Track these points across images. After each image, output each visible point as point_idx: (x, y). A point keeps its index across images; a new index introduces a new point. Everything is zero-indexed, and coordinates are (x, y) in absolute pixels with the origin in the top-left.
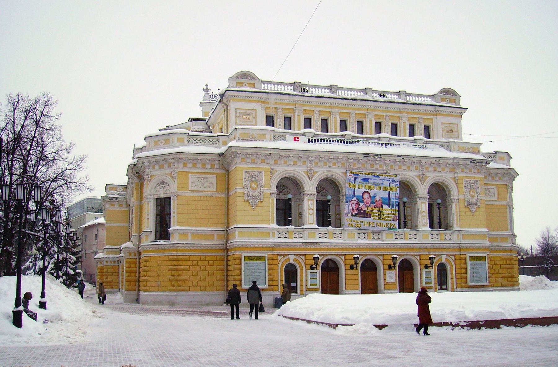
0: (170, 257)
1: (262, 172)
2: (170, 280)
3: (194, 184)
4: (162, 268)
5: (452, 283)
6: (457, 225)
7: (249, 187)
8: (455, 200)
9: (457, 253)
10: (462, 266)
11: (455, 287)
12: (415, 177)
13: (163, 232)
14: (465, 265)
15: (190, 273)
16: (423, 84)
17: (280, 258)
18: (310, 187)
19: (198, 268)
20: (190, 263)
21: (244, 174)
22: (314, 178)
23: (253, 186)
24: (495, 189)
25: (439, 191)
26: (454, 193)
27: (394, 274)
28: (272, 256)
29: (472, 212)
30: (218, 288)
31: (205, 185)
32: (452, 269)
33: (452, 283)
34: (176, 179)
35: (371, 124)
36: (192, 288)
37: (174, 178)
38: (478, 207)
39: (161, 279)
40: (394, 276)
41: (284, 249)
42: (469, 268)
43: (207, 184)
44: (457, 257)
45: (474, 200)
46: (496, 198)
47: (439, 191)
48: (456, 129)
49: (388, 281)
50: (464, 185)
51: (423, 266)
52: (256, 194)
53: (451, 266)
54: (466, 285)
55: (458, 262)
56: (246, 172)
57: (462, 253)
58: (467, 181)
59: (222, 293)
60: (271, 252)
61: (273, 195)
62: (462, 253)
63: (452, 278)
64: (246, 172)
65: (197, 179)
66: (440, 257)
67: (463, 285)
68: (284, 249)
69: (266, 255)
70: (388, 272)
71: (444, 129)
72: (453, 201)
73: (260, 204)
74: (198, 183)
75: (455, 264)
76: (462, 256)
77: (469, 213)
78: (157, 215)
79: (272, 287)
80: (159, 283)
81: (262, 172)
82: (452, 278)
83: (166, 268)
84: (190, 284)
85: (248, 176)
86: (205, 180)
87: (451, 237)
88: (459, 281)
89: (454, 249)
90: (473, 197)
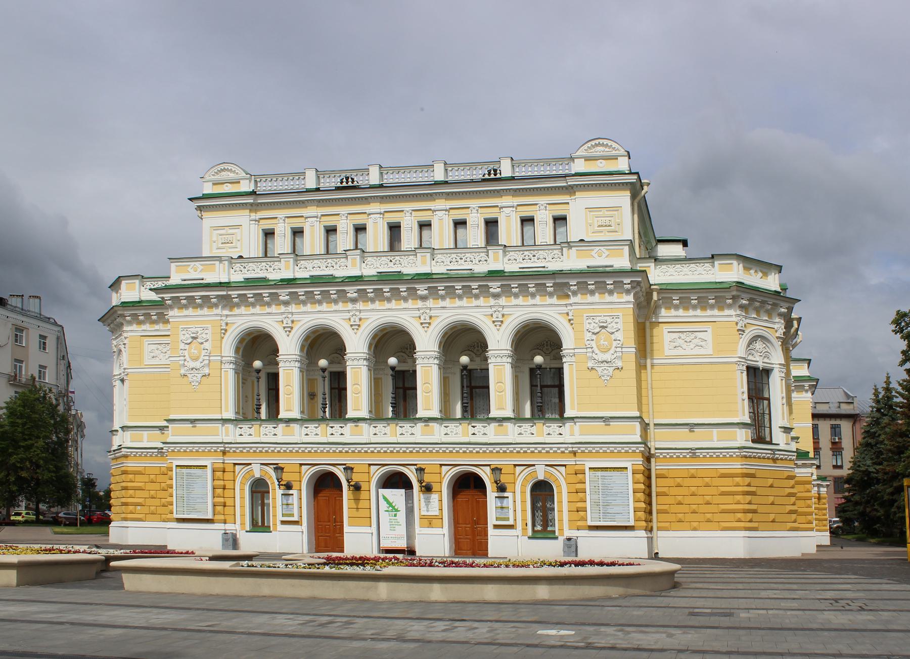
12: (483, 318)
24: (710, 330)
26: (568, 342)
58: (593, 317)
61: (227, 366)
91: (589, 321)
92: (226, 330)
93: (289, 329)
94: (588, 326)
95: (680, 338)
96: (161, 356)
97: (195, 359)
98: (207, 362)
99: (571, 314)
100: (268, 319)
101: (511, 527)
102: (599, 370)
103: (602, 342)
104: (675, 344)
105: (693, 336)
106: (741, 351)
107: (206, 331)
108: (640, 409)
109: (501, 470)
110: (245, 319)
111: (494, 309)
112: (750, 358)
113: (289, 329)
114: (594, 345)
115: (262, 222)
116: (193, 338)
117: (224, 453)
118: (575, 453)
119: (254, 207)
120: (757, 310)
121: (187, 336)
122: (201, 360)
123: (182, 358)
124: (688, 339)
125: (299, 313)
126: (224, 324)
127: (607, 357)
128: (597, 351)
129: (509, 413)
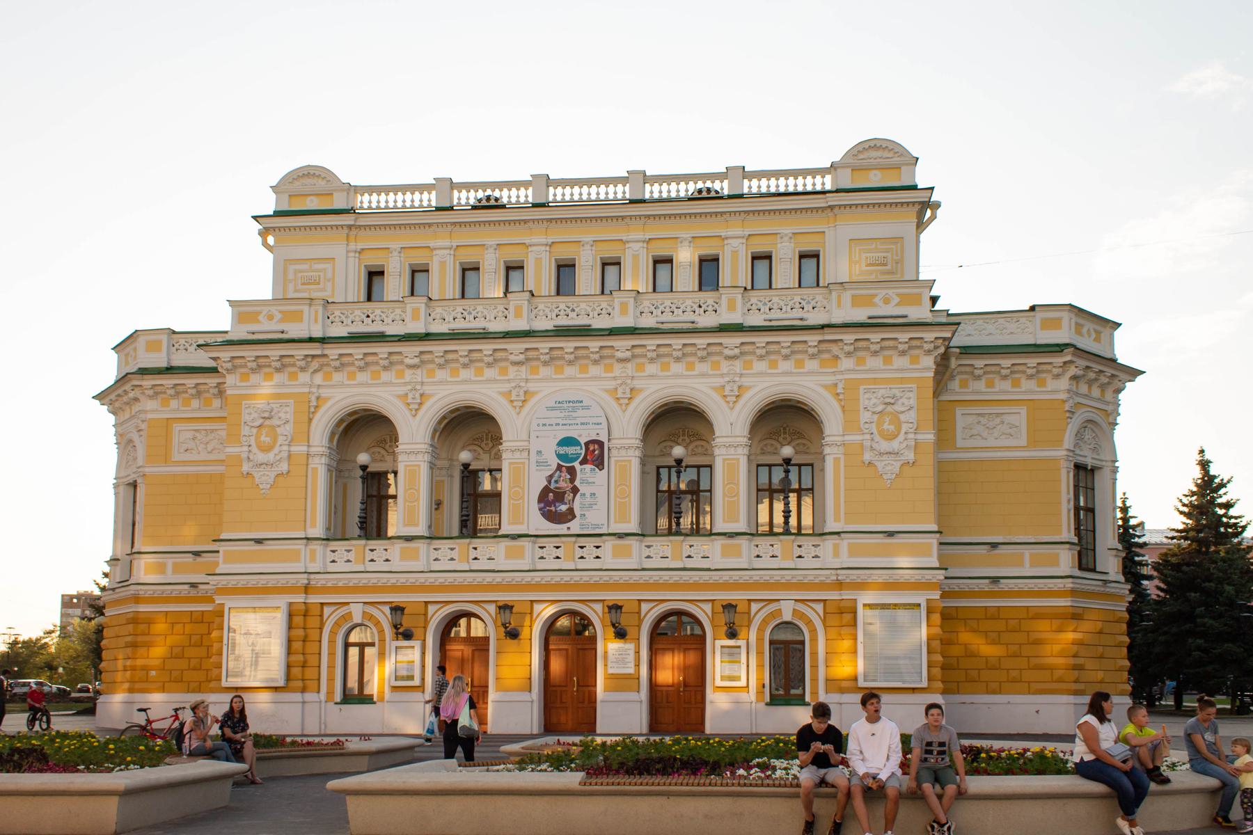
6: (837, 519)
8: (835, 450)
9: (833, 595)
16: (799, 141)
26: (833, 425)
27: (632, 653)
32: (814, 639)
40: (631, 657)
41: (336, 590)
46: (1023, 442)
53: (813, 631)
57: (847, 595)
60: (299, 598)
61: (317, 460)
62: (847, 595)
66: (776, 604)
68: (336, 590)
70: (614, 646)
72: (827, 450)
75: (825, 627)
76: (842, 604)
86: (211, 436)
87: (818, 552)
89: (822, 586)
91: (867, 396)
92: (316, 407)
94: (867, 402)
95: (979, 422)
98: (285, 455)
99: (840, 386)
100: (382, 394)
102: (880, 465)
103: (886, 426)
104: (974, 432)
105: (998, 421)
106: (1068, 440)
108: (940, 518)
109: (735, 607)
110: (346, 392)
111: (727, 379)
112: (1078, 452)
114: (875, 431)
120: (1090, 383)
121: (255, 415)
124: (991, 424)
125: (434, 383)
126: (313, 398)
127: (895, 445)
128: (877, 438)
129: (741, 526)
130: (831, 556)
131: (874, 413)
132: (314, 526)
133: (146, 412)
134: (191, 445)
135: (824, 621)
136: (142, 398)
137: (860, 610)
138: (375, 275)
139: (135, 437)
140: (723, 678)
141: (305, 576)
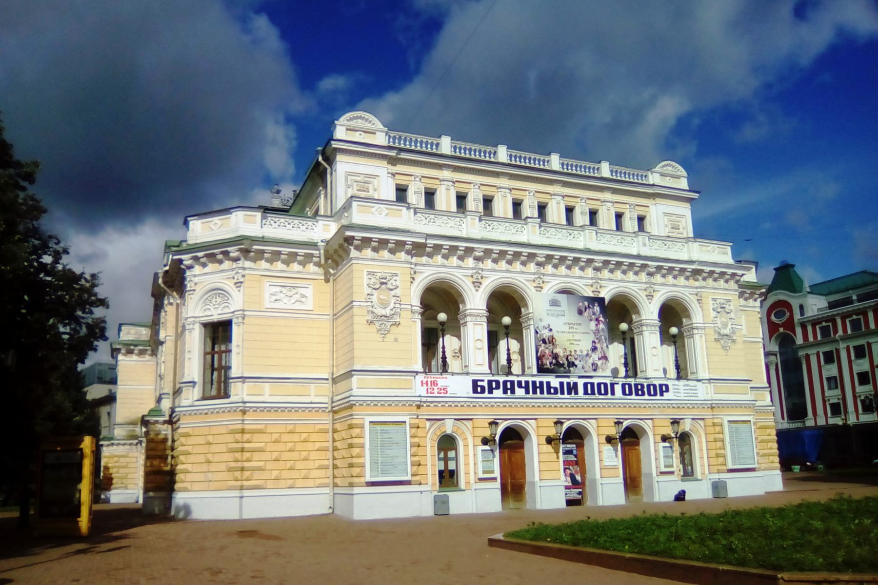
0: (231, 427)
1: (396, 275)
2: (230, 470)
3: (274, 298)
4: (215, 448)
5: (702, 466)
7: (374, 298)
10: (717, 436)
11: (707, 472)
13: (218, 378)
14: (721, 436)
15: (266, 456)
17: (428, 424)
18: (476, 302)
19: (280, 447)
20: (265, 437)
21: (365, 277)
22: (482, 287)
23: (381, 297)
25: (672, 315)
26: (697, 317)
28: (416, 421)
29: (724, 348)
30: (318, 481)
31: (293, 301)
33: (702, 466)
34: (242, 288)
35: (559, 209)
36: (270, 484)
37: (238, 284)
38: (734, 341)
39: (213, 467)
42: (727, 440)
43: (297, 297)
44: (709, 422)
45: (726, 331)
47: (672, 315)
48: (684, 225)
49: (607, 462)
50: (711, 307)
51: (659, 438)
52: (387, 312)
54: (724, 467)
55: (711, 430)
56: (369, 273)
59: (326, 490)
63: (702, 458)
64: (369, 273)
65: (278, 289)
67: (720, 467)
69: (406, 418)
71: (666, 222)
73: (394, 329)
74: (281, 296)
76: (715, 421)
77: (723, 352)
78: (206, 354)
79: (417, 478)
80: (210, 475)
81: (396, 275)
82: (702, 458)
83: (223, 448)
84: (266, 475)
85: (373, 280)
86: (294, 291)
88: (713, 461)
90: (725, 326)
93: (477, 284)
96: (285, 300)
97: (384, 305)
101: (672, 473)
103: (723, 319)
107: (395, 278)
110: (431, 270)
113: (477, 284)
115: (397, 177)
116: (382, 283)
117: (419, 407)
118: (712, 408)
119: (393, 161)
122: (392, 306)
123: (369, 304)
130: (704, 392)
131: (718, 312)
132: (416, 363)
133: (244, 269)
134: (281, 296)
135: (705, 430)
136: (242, 258)
137: (726, 424)
138: (401, 192)
139: (229, 286)
140: (666, 466)
141: (419, 399)
